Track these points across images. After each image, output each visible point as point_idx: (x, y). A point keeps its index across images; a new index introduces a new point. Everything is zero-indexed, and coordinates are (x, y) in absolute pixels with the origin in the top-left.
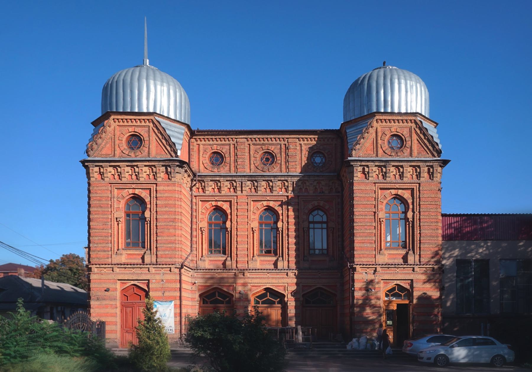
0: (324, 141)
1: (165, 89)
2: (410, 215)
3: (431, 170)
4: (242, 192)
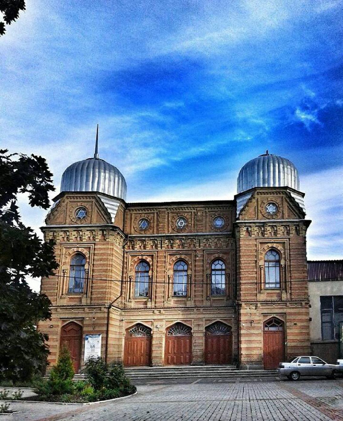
0: (223, 208)
1: (107, 175)
2: (282, 262)
3: (298, 228)
4: (161, 248)
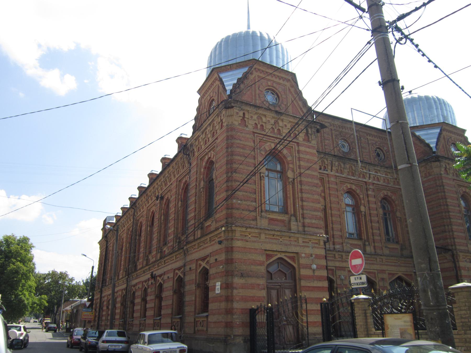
4: (331, 171)
